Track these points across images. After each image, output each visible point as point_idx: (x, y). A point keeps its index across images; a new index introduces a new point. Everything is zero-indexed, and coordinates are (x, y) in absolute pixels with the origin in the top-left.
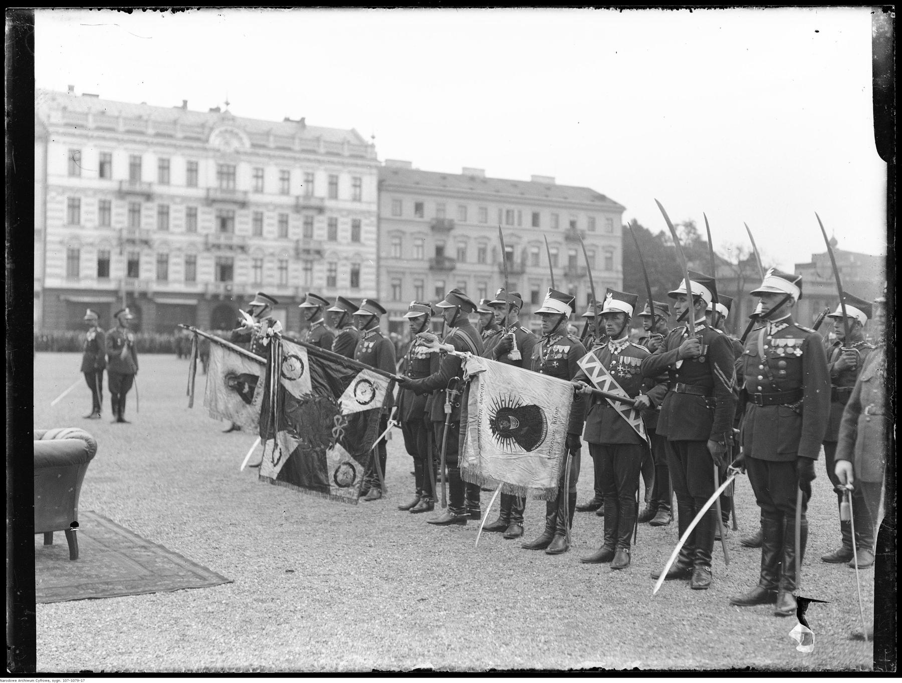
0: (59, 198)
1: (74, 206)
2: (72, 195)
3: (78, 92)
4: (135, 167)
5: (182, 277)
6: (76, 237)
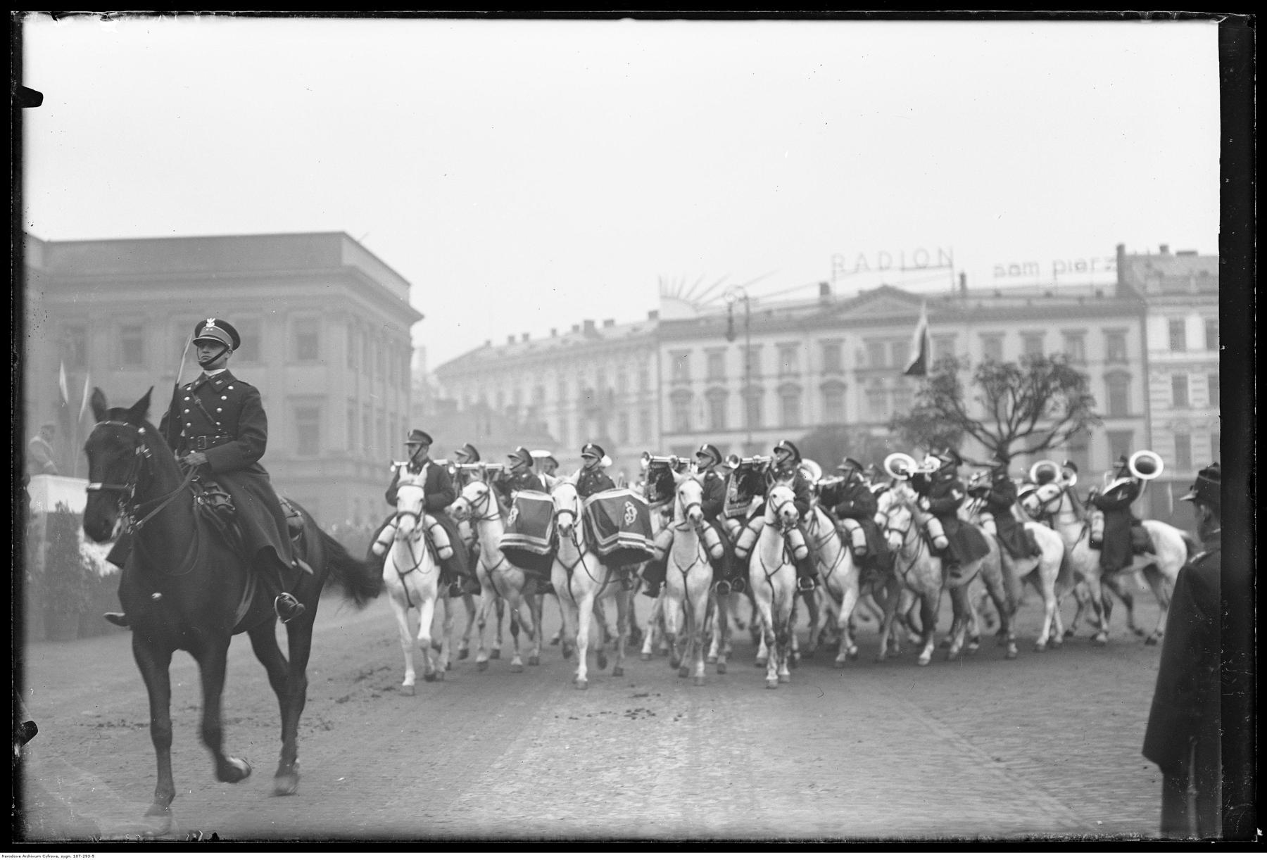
0: (1162, 378)
1: (1179, 385)
2: (1176, 372)
3: (1172, 251)
6: (1184, 421)
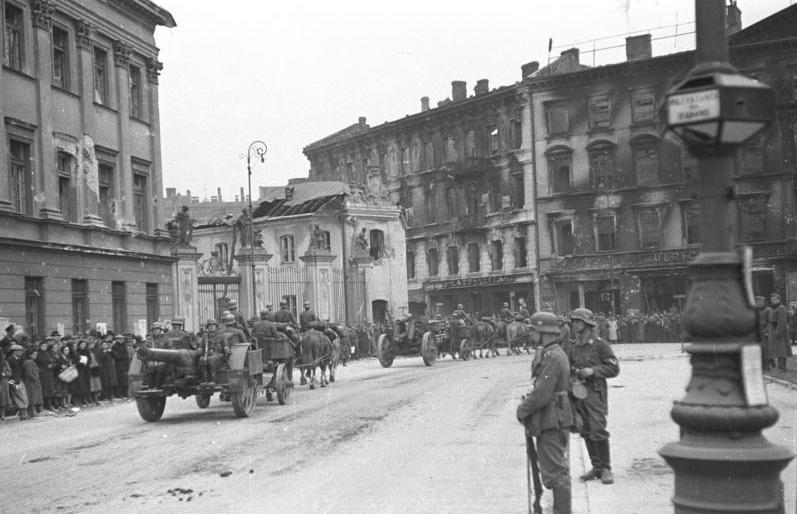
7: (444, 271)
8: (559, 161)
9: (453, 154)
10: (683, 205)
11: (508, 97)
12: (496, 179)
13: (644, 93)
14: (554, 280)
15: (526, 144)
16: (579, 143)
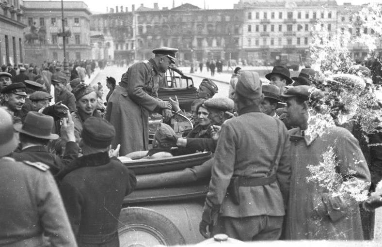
4: (265, 15)
5: (277, 44)
7: (119, 49)
8: (141, 29)
9: (117, 24)
10: (164, 39)
11: (130, 14)
12: (127, 32)
13: (157, 18)
14: (139, 52)
15: (134, 24)
16: (144, 25)
